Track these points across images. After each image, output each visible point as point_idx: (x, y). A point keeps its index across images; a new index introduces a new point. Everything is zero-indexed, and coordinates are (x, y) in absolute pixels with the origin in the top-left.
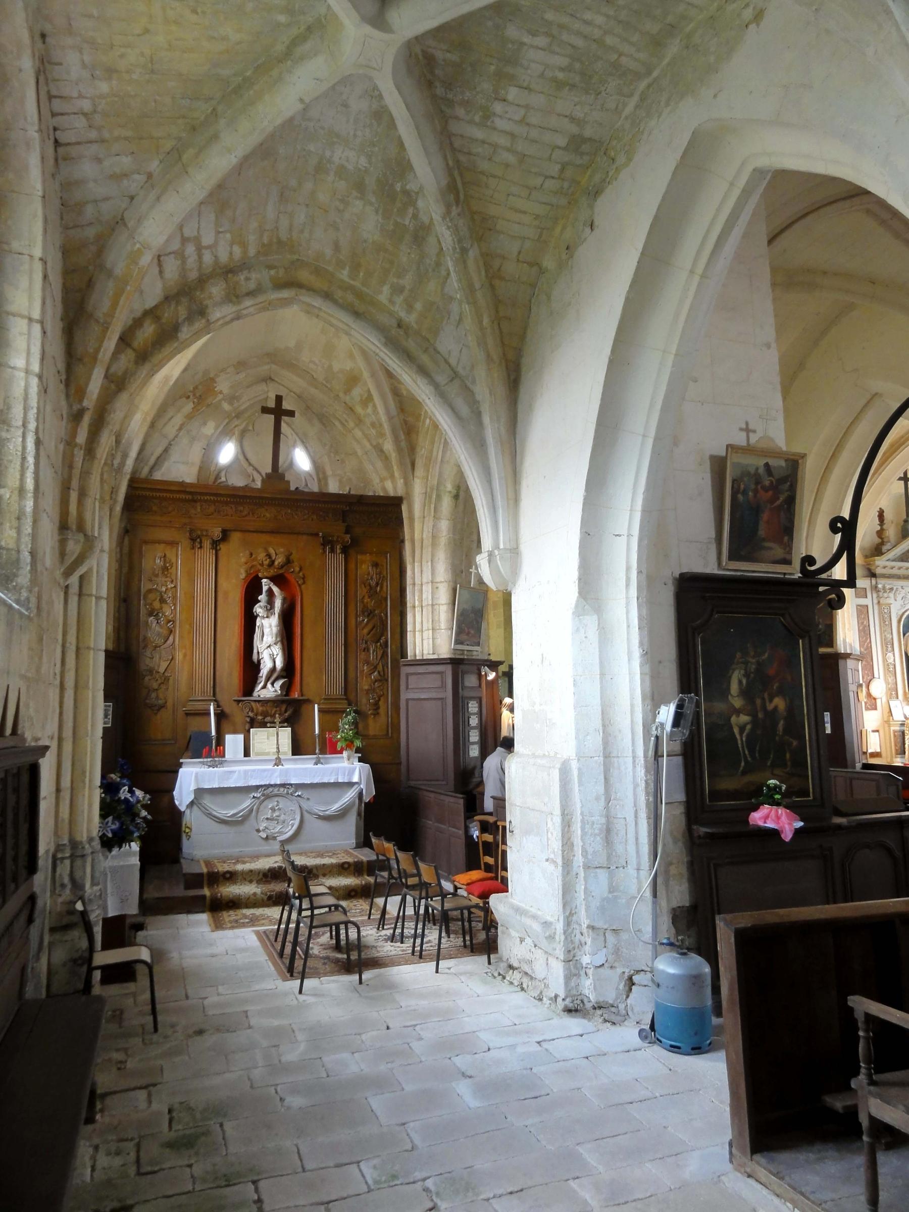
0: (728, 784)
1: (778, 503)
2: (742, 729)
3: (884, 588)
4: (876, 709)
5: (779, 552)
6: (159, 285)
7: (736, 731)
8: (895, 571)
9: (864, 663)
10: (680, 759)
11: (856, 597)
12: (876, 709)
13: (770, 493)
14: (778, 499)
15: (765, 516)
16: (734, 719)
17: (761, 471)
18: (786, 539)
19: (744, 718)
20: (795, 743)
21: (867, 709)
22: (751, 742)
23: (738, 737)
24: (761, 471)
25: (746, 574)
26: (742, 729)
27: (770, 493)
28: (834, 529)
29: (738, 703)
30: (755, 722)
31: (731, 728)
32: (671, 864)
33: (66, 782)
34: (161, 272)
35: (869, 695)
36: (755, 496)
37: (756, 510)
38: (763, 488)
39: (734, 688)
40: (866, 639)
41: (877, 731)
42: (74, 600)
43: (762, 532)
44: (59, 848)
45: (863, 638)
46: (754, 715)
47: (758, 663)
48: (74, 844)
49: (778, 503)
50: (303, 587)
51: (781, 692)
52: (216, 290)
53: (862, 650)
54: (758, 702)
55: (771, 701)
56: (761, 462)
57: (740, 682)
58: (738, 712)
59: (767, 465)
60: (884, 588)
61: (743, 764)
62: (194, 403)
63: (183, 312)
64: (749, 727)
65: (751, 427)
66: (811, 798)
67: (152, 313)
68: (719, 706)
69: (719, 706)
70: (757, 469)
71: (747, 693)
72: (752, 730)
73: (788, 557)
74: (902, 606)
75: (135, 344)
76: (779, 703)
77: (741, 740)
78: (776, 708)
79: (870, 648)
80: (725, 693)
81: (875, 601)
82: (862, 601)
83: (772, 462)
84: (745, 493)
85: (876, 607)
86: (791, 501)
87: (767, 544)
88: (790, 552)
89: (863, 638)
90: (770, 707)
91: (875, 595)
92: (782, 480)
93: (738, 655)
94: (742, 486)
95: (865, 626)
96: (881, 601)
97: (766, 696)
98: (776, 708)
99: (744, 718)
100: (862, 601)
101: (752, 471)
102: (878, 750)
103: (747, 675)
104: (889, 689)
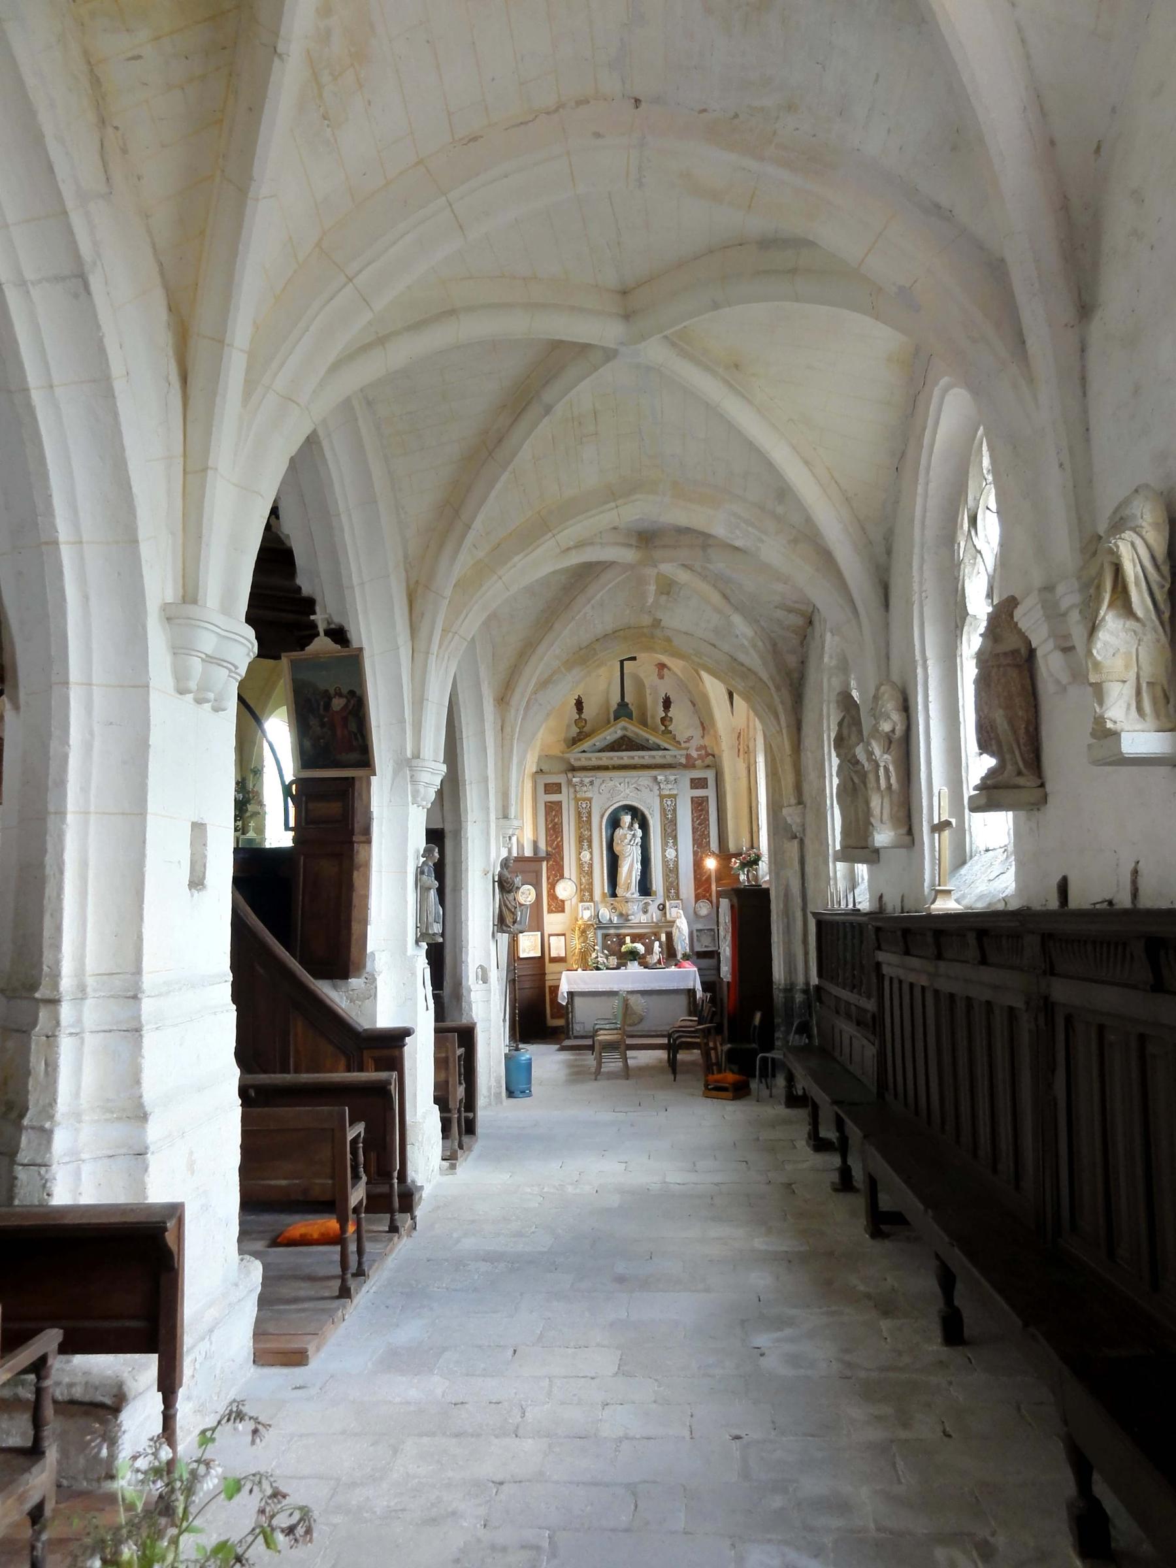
3: (582, 782)
4: (563, 911)
8: (604, 762)
9: (551, 863)
11: (546, 794)
12: (563, 911)
21: (550, 911)
35: (552, 896)
40: (557, 837)
41: (564, 935)
45: (551, 836)
53: (550, 849)
60: (582, 782)
74: (608, 799)
79: (559, 848)
81: (572, 796)
82: (554, 798)
85: (572, 803)
89: (551, 836)
91: (572, 790)
95: (556, 824)
96: (578, 796)
100: (554, 798)
102: (563, 955)
104: (581, 890)
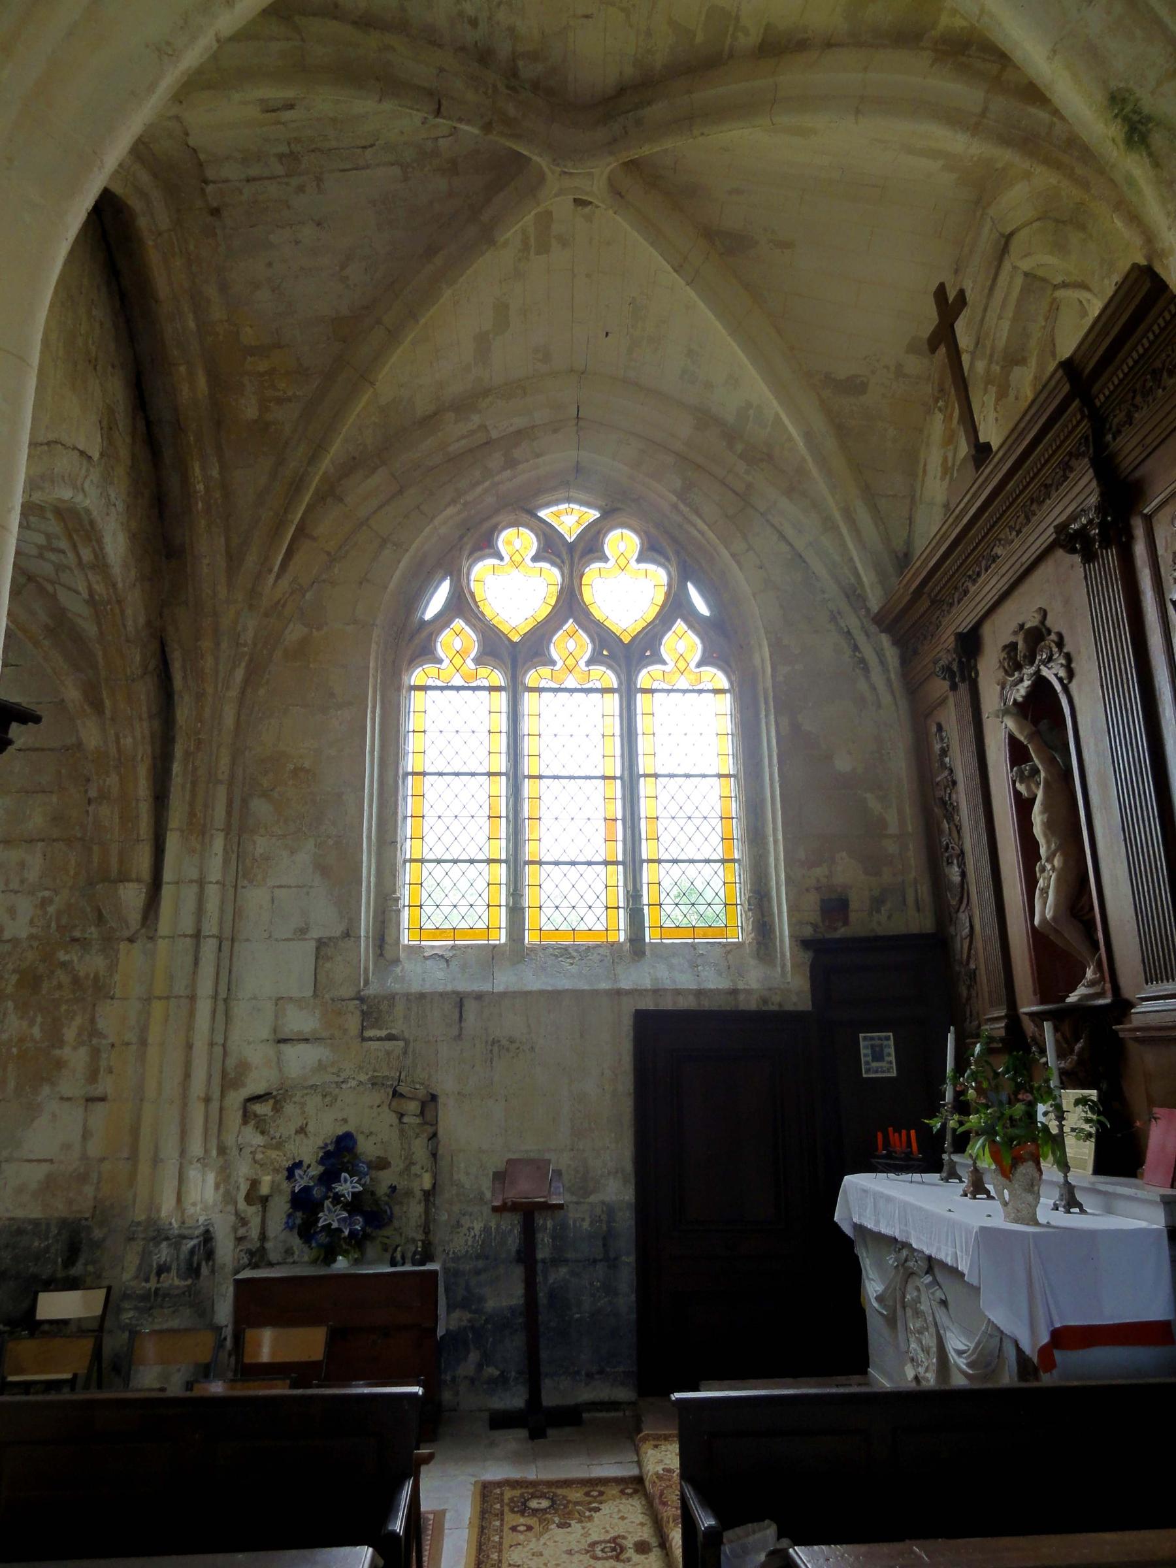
50: (1073, 687)
62: (940, 410)
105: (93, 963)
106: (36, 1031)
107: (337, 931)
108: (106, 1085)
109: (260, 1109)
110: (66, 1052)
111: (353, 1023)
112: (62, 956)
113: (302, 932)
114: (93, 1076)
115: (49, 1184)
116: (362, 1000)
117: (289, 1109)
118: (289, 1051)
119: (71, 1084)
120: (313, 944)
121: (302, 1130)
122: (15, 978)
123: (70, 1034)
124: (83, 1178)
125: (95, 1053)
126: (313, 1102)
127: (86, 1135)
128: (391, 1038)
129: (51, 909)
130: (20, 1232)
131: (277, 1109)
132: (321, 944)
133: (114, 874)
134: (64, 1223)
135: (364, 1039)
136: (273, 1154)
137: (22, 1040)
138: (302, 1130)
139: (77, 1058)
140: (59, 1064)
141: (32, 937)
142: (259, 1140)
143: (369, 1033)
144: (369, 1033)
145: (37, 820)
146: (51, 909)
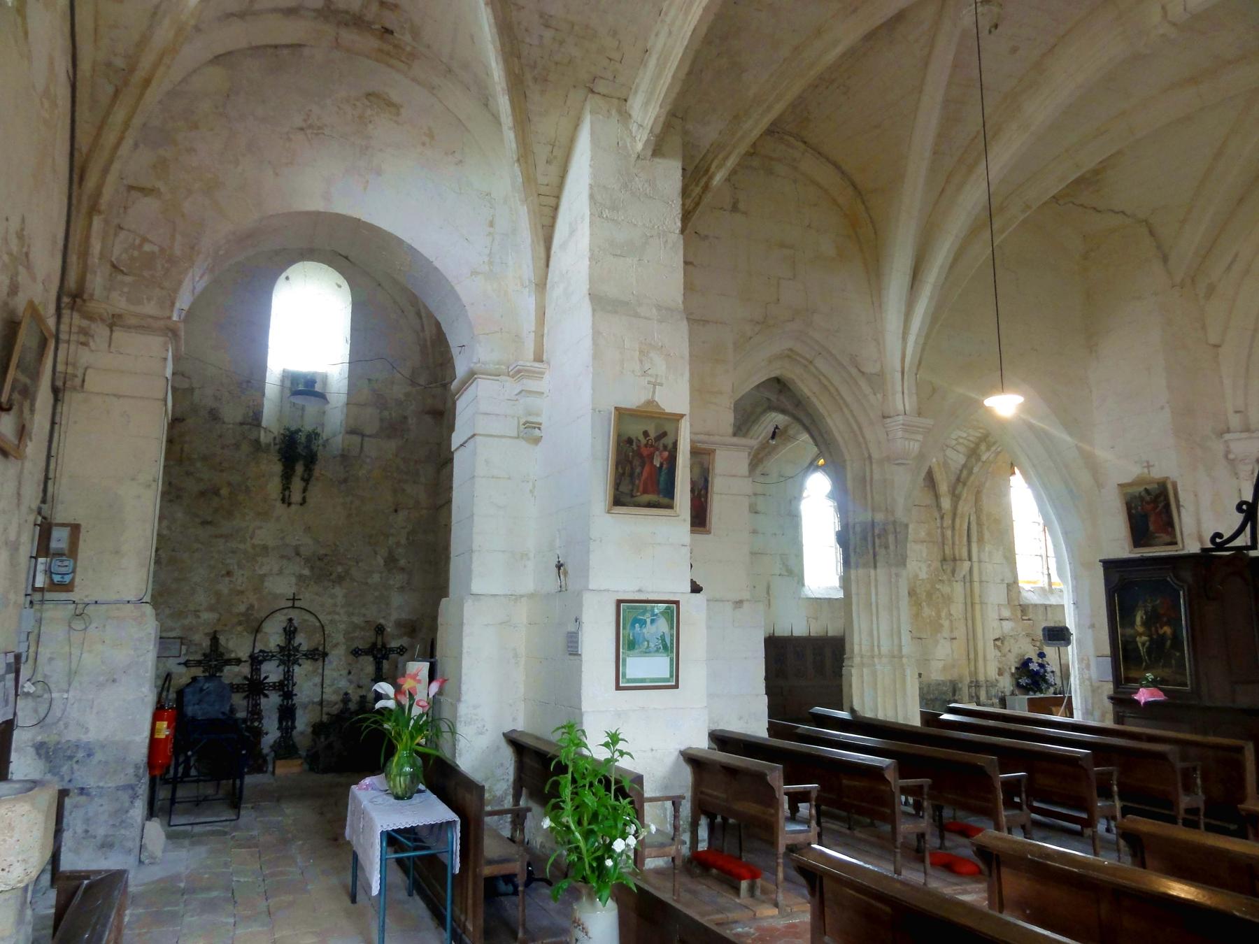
0: (1133, 674)
1: (1158, 510)
2: (1143, 644)
5: (1167, 539)
6: (961, 456)
7: (1140, 645)
10: (1109, 659)
13: (1152, 505)
14: (1158, 507)
15: (1152, 519)
16: (1138, 639)
17: (1143, 494)
18: (1170, 529)
19: (1144, 638)
20: (1178, 654)
22: (1149, 652)
23: (1141, 648)
24: (1143, 494)
25: (1145, 555)
26: (1143, 644)
27: (1152, 505)
28: (1239, 508)
29: (1140, 629)
30: (1151, 640)
31: (1136, 642)
32: (1107, 712)
33: (972, 656)
34: (957, 451)
36: (1142, 509)
37: (1145, 517)
38: (1148, 503)
39: (1138, 620)
42: (968, 584)
43: (1152, 528)
44: (971, 682)
46: (1150, 636)
47: (1153, 607)
48: (977, 681)
49: (1158, 510)
51: (1168, 623)
52: (983, 447)
54: (1153, 629)
55: (1162, 628)
56: (1142, 489)
57: (1142, 618)
58: (1141, 635)
59: (1146, 490)
61: (1144, 664)
63: (973, 460)
64: (1148, 643)
65: (1151, 463)
66: (1188, 688)
67: (964, 466)
68: (1129, 631)
69: (1129, 631)
70: (1140, 493)
71: (1144, 624)
72: (1150, 645)
73: (1174, 540)
75: (962, 480)
76: (1167, 630)
77: (1143, 650)
78: (1165, 633)
80: (1133, 624)
83: (1147, 487)
84: (1136, 508)
86: (1167, 506)
87: (1157, 535)
88: (1175, 536)
90: (1161, 632)
92: (1157, 497)
93: (1140, 603)
94: (1133, 505)
97: (1158, 625)
98: (1165, 633)
99: (1144, 638)
101: (1137, 495)
103: (1146, 613)
105: (946, 589)
106: (933, 613)
107: (1011, 581)
108: (956, 634)
109: (998, 643)
110: (942, 622)
111: (1019, 614)
112: (937, 586)
113: (1003, 580)
114: (952, 631)
115: (944, 668)
116: (1020, 605)
117: (1006, 643)
118: (1004, 623)
119: (946, 633)
120: (1005, 585)
121: (1010, 651)
122: (925, 594)
123: (943, 614)
124: (953, 666)
125: (951, 621)
126: (1012, 641)
127: (953, 652)
128: (1029, 620)
129: (932, 568)
130: (939, 684)
131: (1002, 643)
132: (1008, 585)
133: (957, 558)
134: (951, 681)
135: (1023, 620)
136: (1004, 658)
137: (930, 617)
138: (1010, 651)
139: (946, 623)
140: (941, 626)
141: (928, 579)
142: (999, 654)
143: (1024, 618)
144: (1024, 618)
145: (923, 534)
146: (932, 568)
